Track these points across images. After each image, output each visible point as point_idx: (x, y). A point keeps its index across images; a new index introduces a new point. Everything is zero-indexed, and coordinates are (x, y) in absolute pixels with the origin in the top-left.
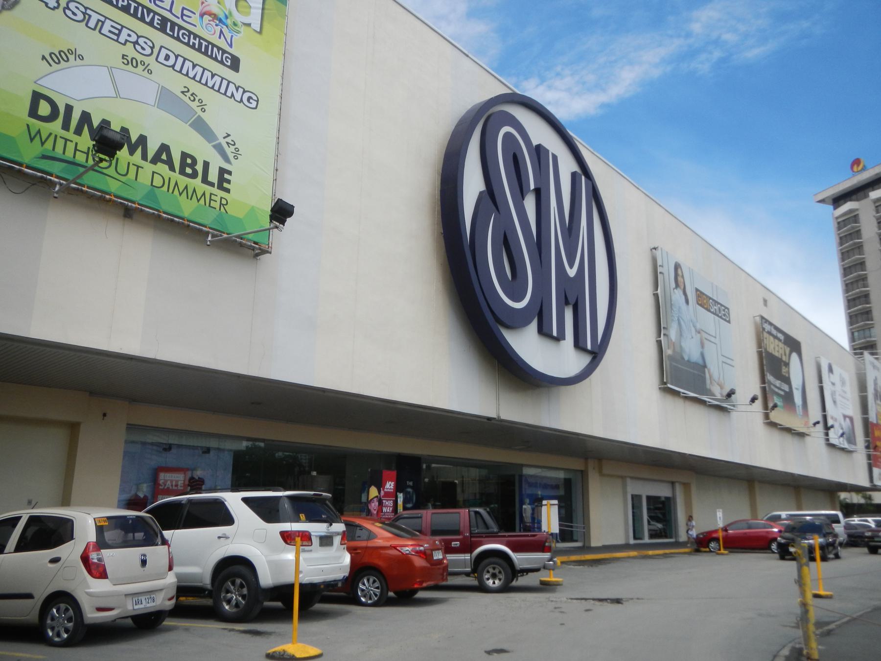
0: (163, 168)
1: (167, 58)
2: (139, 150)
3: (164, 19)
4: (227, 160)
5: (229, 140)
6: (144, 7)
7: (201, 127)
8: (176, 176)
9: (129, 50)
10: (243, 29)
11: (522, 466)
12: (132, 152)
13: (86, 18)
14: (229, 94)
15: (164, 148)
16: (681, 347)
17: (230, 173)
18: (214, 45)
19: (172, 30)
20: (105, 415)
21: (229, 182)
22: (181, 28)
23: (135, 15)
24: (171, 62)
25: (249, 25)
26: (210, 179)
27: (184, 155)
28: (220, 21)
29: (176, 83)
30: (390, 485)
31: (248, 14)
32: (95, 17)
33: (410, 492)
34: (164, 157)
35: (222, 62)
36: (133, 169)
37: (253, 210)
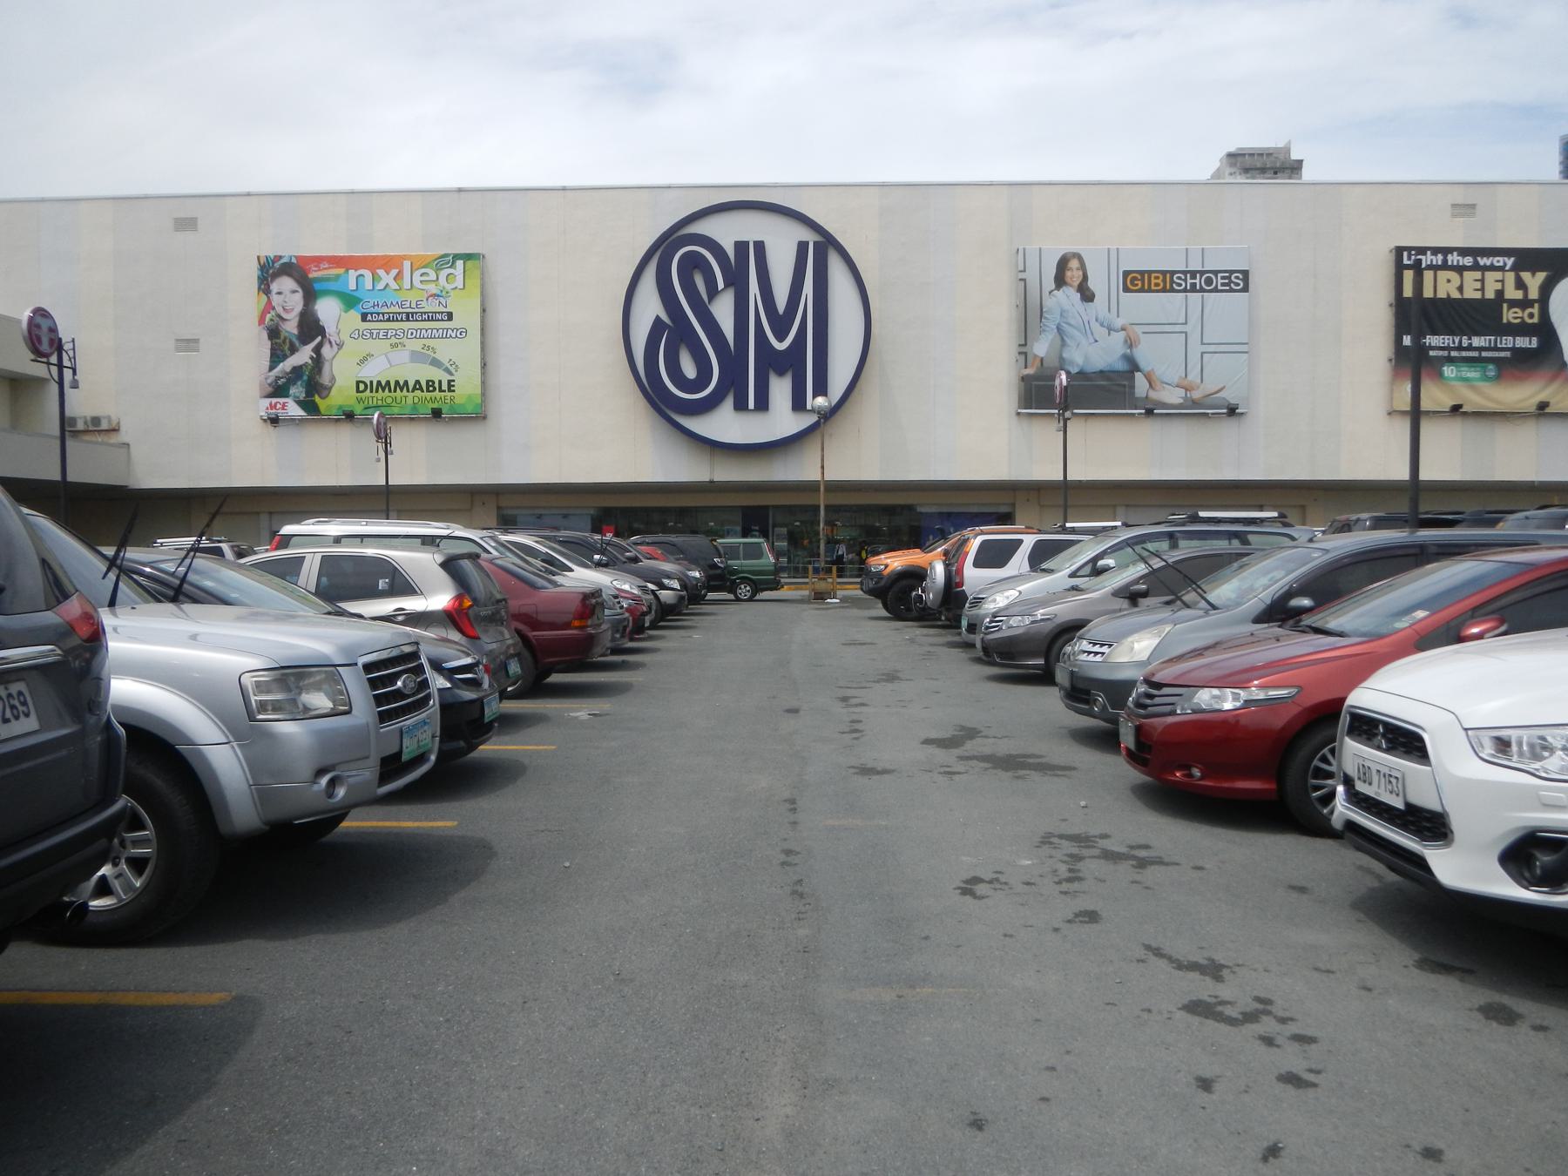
0: (418, 393)
1: (412, 334)
2: (405, 389)
3: (408, 314)
4: (451, 374)
5: (451, 363)
6: (396, 313)
7: (436, 363)
8: (426, 394)
9: (394, 340)
10: (452, 293)
12: (402, 391)
13: (372, 334)
14: (448, 336)
15: (418, 382)
17: (454, 381)
18: (436, 313)
19: (412, 317)
20: (484, 504)
21: (453, 386)
22: (416, 313)
23: (393, 321)
24: (414, 335)
25: (456, 288)
26: (443, 388)
27: (428, 382)
28: (438, 296)
29: (416, 345)
31: (455, 280)
32: (375, 332)
34: (418, 387)
35: (442, 320)
36: (404, 399)
37: (470, 397)
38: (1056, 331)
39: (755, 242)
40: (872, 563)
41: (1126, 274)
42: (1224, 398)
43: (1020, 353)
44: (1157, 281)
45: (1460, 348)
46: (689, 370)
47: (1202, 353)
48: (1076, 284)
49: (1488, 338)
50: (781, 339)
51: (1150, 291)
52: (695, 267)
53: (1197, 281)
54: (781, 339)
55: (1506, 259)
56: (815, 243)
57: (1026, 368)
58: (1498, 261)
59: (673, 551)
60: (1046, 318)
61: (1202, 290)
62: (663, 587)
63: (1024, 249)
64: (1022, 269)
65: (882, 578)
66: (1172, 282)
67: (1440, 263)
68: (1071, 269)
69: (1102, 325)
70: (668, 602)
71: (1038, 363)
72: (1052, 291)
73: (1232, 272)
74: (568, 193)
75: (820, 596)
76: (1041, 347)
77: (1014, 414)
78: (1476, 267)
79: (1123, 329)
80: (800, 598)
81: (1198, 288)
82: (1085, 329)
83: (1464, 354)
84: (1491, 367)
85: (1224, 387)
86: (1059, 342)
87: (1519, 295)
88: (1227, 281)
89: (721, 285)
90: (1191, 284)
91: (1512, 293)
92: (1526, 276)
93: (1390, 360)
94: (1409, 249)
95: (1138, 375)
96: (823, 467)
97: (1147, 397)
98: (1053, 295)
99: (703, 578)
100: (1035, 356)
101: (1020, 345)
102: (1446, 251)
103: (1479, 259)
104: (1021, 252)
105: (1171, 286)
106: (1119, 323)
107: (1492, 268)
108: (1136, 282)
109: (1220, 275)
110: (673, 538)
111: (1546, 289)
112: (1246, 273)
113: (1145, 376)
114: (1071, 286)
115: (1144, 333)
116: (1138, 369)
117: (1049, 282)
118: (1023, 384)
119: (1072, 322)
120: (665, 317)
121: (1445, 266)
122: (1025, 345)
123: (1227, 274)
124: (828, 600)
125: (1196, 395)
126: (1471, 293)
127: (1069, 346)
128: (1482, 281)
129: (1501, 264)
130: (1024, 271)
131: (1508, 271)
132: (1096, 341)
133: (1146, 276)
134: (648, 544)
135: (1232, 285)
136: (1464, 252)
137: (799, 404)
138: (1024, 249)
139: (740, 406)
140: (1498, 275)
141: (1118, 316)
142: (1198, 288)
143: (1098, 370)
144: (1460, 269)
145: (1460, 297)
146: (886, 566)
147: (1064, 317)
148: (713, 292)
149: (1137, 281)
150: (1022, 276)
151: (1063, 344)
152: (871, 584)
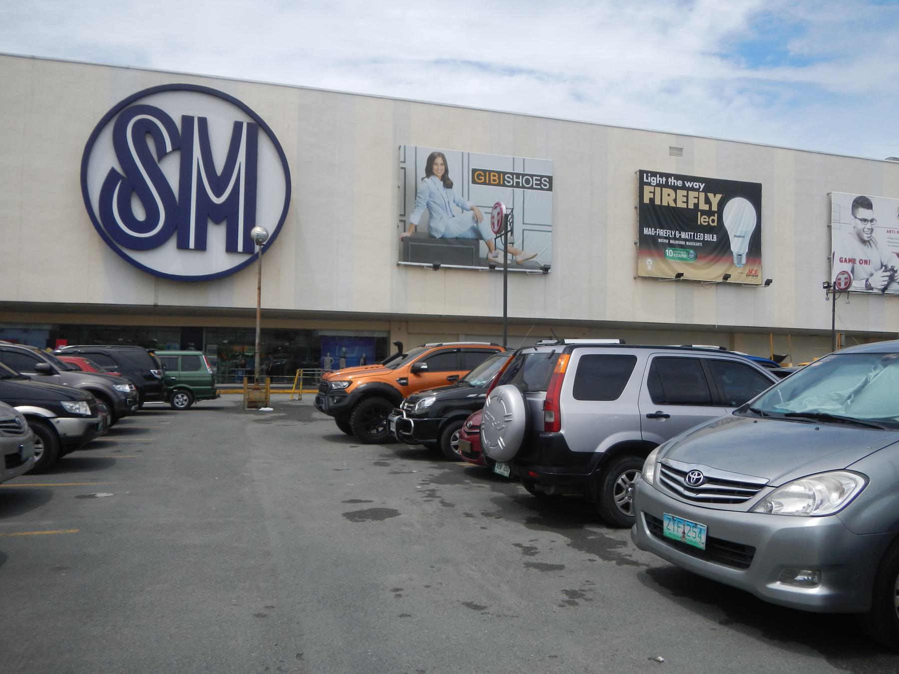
16: (430, 227)
38: (426, 206)
40: (332, 379)
41: (474, 171)
42: (537, 262)
43: (401, 221)
44: (494, 178)
45: (675, 238)
46: (139, 214)
47: (523, 230)
48: (440, 175)
49: (690, 233)
50: (218, 194)
51: (489, 184)
52: (148, 132)
53: (520, 180)
54: (218, 194)
55: (700, 184)
56: (248, 124)
57: (405, 231)
58: (696, 185)
59: (100, 363)
60: (419, 197)
61: (523, 187)
62: (61, 412)
63: (405, 146)
65: (346, 396)
66: (504, 179)
67: (664, 183)
68: (437, 164)
69: (458, 205)
70: (69, 434)
71: (413, 229)
72: (424, 178)
73: (542, 177)
74: (36, 62)
75: (253, 405)
76: (416, 218)
77: (395, 264)
78: (684, 188)
79: (472, 209)
80: (233, 405)
81: (521, 185)
82: (446, 207)
83: (677, 242)
84: (692, 252)
85: (537, 254)
86: (428, 215)
87: (706, 207)
88: (539, 182)
89: (169, 148)
90: (517, 182)
91: (703, 206)
92: (711, 195)
93: (635, 243)
94: (647, 172)
95: (482, 242)
96: (259, 289)
97: (487, 258)
98: (424, 181)
99: (135, 393)
100: (411, 224)
101: (401, 215)
102: (668, 176)
103: (686, 182)
104: (402, 149)
105: (504, 182)
106: (469, 204)
107: (693, 189)
108: (481, 177)
109: (534, 178)
110: (108, 349)
111: (722, 205)
112: (550, 178)
113: (486, 243)
114: (437, 176)
115: (486, 213)
116: (482, 238)
117: (422, 173)
118: (402, 243)
119: (437, 201)
120: (119, 169)
121: (667, 186)
122: (404, 215)
123: (539, 178)
124: (263, 409)
125: (519, 258)
126: (681, 205)
127: (434, 218)
128: (687, 197)
129: (698, 187)
130: (404, 162)
131: (701, 192)
132: (453, 216)
133: (487, 173)
134: (80, 354)
135: (542, 185)
136: (678, 177)
137: (231, 247)
138: (405, 146)
139: (183, 245)
140: (696, 194)
141: (469, 200)
142: (521, 185)
143: (455, 236)
144: (675, 188)
145: (675, 206)
146: (350, 383)
147: (432, 197)
148: (162, 154)
149: (481, 177)
150: (402, 165)
151: (431, 216)
152: (332, 403)
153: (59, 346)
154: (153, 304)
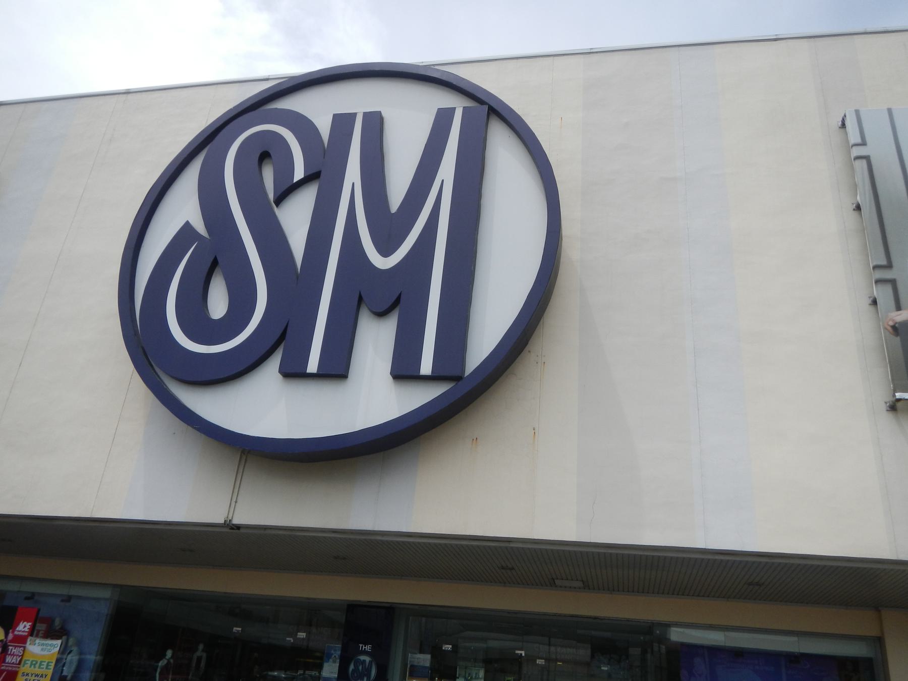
11: (667, 625)
30: (25, 627)
33: (364, 661)
39: (366, 115)
50: (385, 252)
54: (385, 252)
57: (899, 308)
63: (857, 112)
64: (859, 140)
74: (130, 96)
77: (884, 407)
120: (199, 226)
122: (889, 266)
130: (864, 143)
138: (857, 112)
150: (856, 152)
153: (18, 625)
154: (221, 521)
